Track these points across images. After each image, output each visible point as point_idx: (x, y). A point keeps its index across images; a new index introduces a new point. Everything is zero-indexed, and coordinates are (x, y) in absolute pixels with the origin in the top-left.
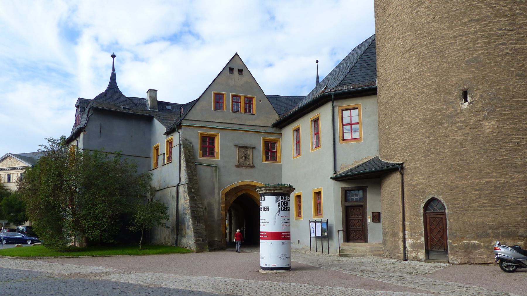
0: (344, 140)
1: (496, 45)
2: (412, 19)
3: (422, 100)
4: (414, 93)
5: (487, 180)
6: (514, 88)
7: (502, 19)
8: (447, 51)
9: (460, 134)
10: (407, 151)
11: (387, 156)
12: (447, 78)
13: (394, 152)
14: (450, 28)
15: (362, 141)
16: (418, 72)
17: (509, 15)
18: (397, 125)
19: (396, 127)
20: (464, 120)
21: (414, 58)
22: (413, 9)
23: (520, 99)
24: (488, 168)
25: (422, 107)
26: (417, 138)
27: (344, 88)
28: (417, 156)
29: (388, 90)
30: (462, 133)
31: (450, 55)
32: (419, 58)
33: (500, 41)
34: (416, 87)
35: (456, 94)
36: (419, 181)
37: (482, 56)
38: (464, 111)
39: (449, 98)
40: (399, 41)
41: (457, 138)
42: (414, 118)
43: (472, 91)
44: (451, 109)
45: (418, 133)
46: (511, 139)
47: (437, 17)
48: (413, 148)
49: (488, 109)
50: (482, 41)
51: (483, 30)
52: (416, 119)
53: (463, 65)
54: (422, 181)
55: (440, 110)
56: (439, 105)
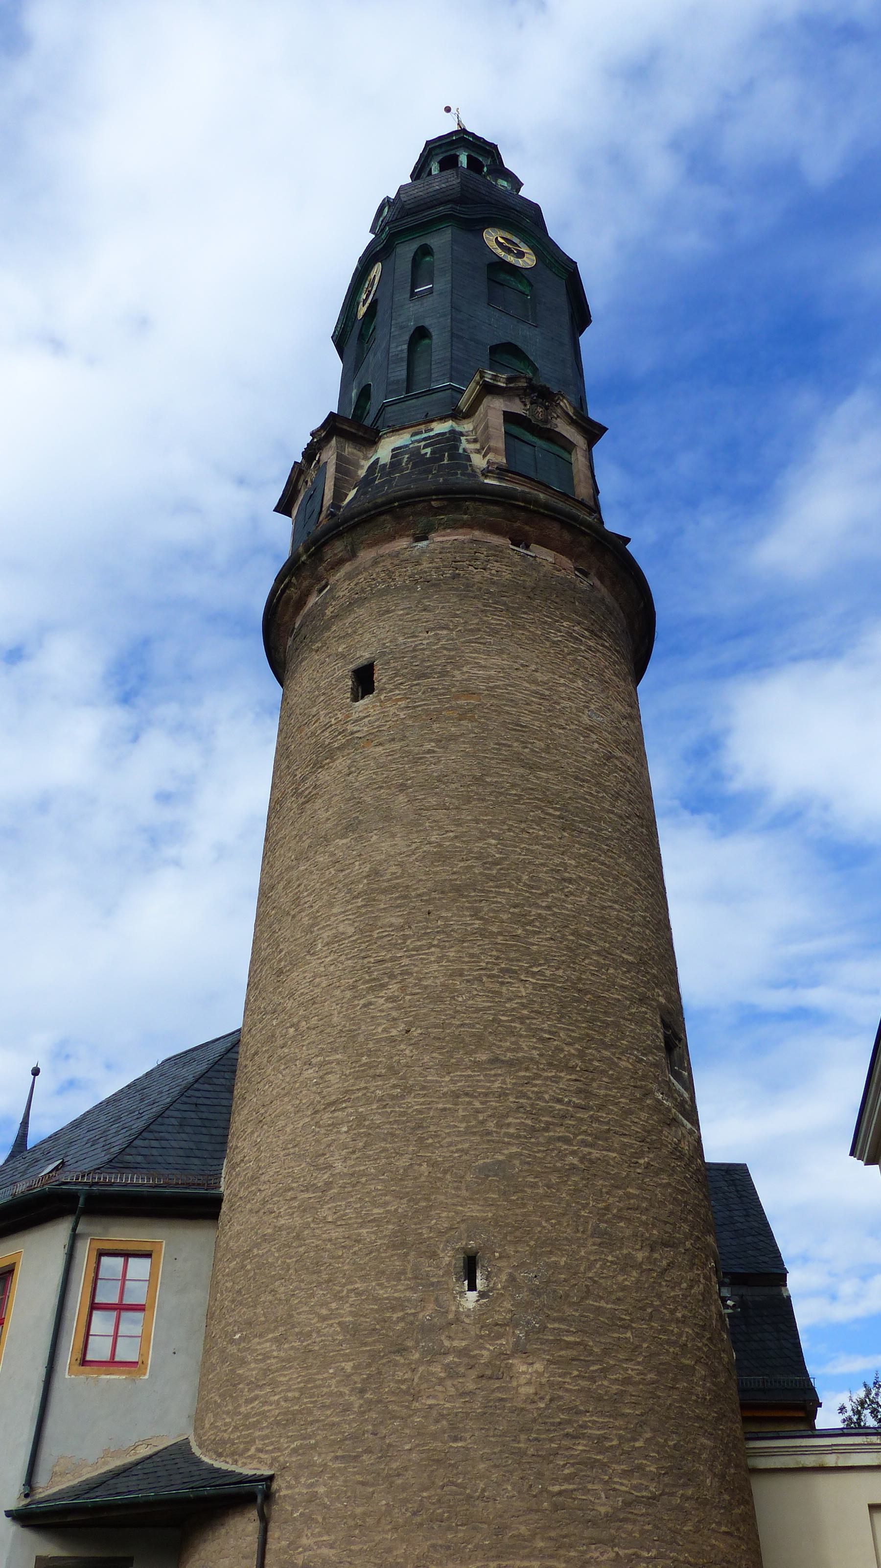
0: (84, 1362)
1: (550, 1140)
2: (352, 1019)
3: (354, 1264)
4: (334, 1235)
6: (589, 1268)
7: (562, 1074)
8: (432, 1128)
9: (452, 1391)
10: (292, 1430)
11: (223, 1442)
12: (426, 1207)
13: (248, 1429)
14: (445, 1067)
15: (145, 1374)
16: (352, 1175)
17: (578, 1069)
18: (270, 1336)
19: (266, 1341)
20: (465, 1348)
21: (345, 1129)
22: (356, 994)
23: (603, 1304)
24: (521, 1519)
25: (352, 1287)
26: (325, 1390)
27: (121, 1179)
28: (320, 1454)
29: (257, 1212)
30: (457, 1389)
31: (439, 1142)
32: (359, 1134)
34: (340, 1218)
35: (447, 1259)
36: (319, 1551)
37: (517, 1162)
38: (468, 1316)
39: (429, 1269)
40: (310, 1071)
41: (442, 1403)
42: (324, 1319)
43: (489, 1261)
44: (431, 1306)
45: (331, 1371)
46: (581, 1427)
47: (416, 1032)
48: (311, 1423)
49: (528, 1323)
50: (519, 1121)
51: (521, 1092)
52: (330, 1322)
53: (469, 1177)
54: (325, 1551)
55: (398, 1305)
56: (399, 1287)
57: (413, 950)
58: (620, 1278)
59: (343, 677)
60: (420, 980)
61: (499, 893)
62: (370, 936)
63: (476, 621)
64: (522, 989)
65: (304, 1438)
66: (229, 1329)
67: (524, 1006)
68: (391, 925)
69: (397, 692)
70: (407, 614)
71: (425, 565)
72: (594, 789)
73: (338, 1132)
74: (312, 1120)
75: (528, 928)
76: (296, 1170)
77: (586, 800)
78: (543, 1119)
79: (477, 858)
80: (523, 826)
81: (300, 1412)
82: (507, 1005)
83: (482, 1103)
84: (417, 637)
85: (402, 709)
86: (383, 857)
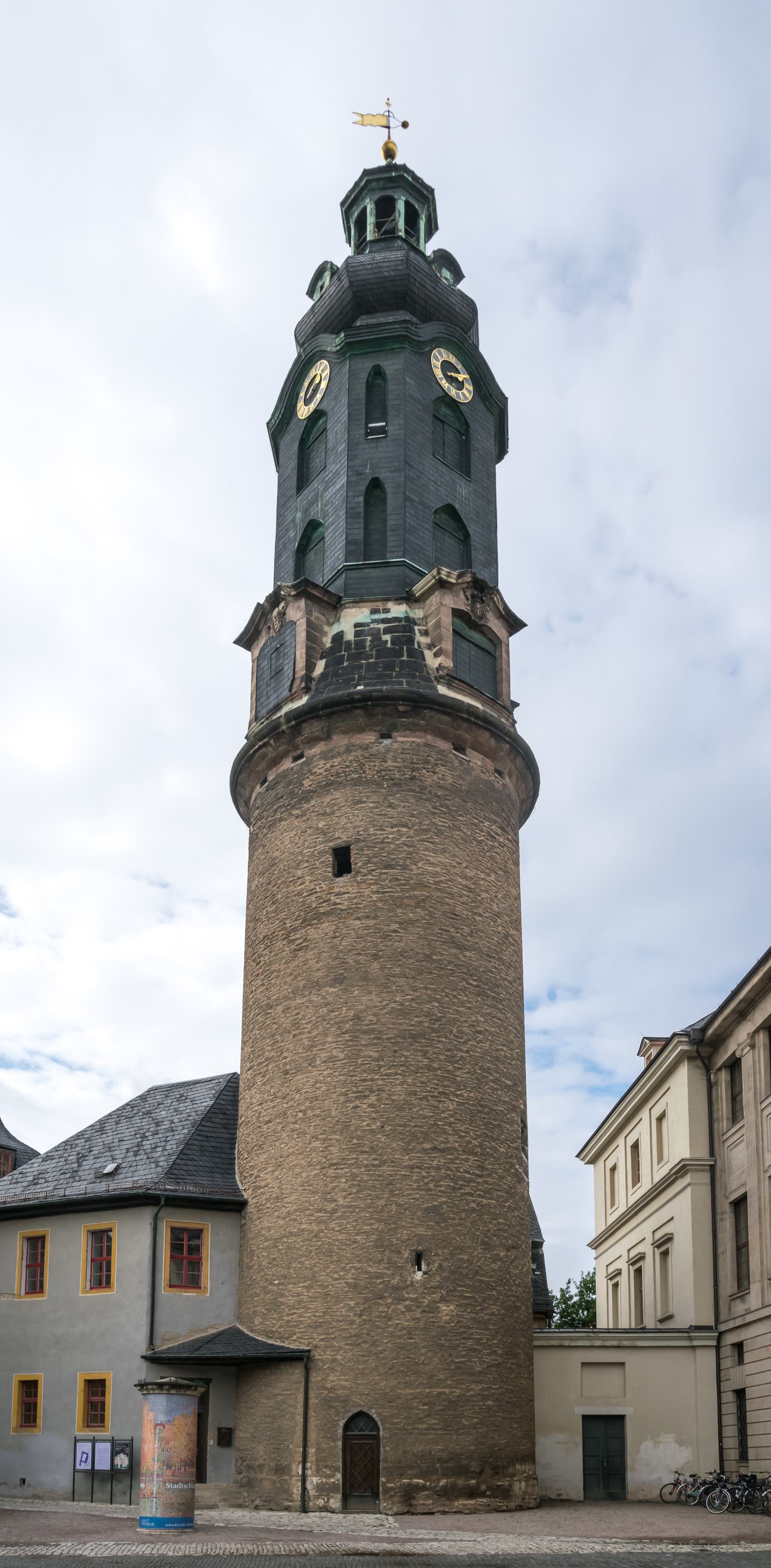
1: (463, 1194)
2: (346, 1115)
4: (340, 1238)
6: (478, 1261)
7: (470, 1157)
8: (398, 1185)
9: (408, 1317)
10: (319, 1330)
14: (406, 1151)
16: (350, 1207)
18: (301, 1285)
23: (484, 1278)
26: (339, 1313)
28: (337, 1342)
32: (353, 1184)
33: (466, 1188)
34: (343, 1229)
35: (406, 1255)
37: (445, 1206)
38: (417, 1283)
42: (336, 1279)
43: (429, 1256)
49: (448, 1287)
51: (448, 1167)
53: (419, 1213)
55: (380, 1276)
57: (385, 1075)
58: (493, 1266)
60: (390, 1095)
61: (439, 1041)
62: (356, 1062)
63: (427, 822)
64: (451, 1105)
65: (328, 1334)
67: (451, 1116)
68: (370, 1057)
69: (370, 877)
70: (377, 808)
71: (390, 763)
72: (497, 963)
73: (340, 1182)
74: (321, 1172)
75: (455, 1065)
76: (312, 1199)
77: (492, 972)
78: (460, 1183)
79: (426, 1016)
80: (455, 993)
81: (325, 1322)
82: (442, 1115)
83: (427, 1173)
84: (384, 830)
86: (363, 1007)
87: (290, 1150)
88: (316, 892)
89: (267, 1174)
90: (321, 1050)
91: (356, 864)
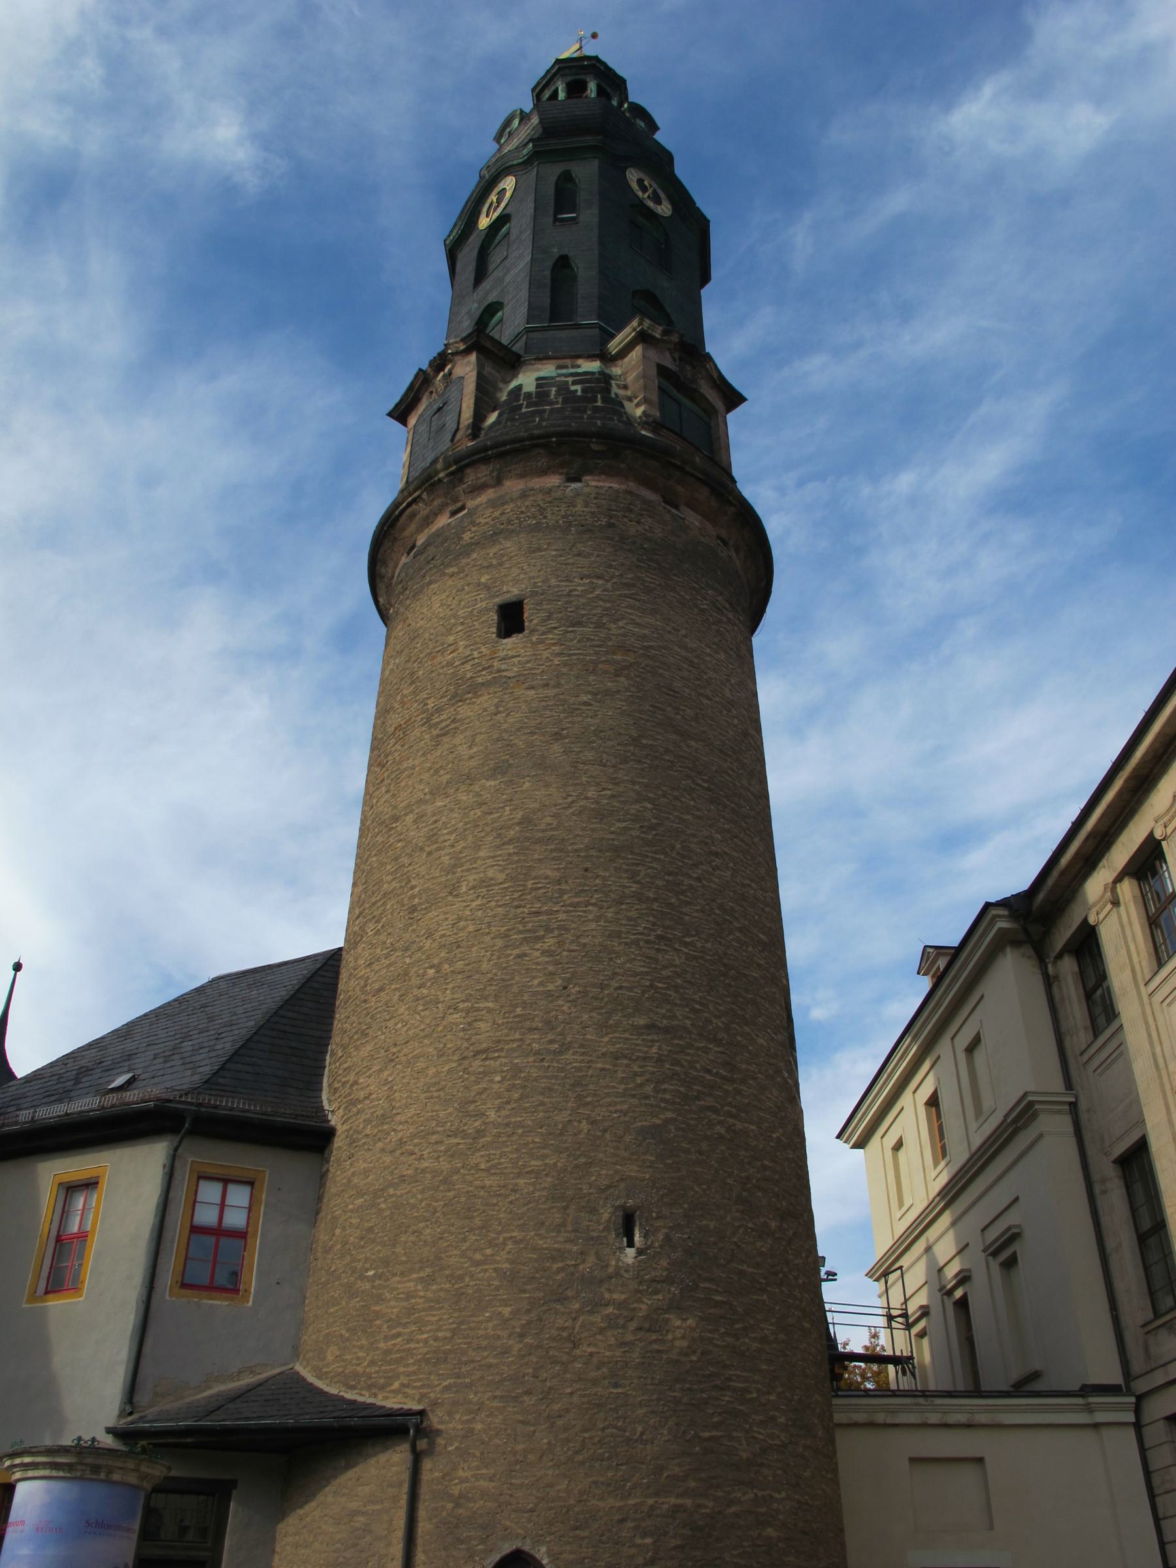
2: (505, 968)
3: (510, 1213)
4: (488, 1183)
5: (673, 1501)
7: (711, 1046)
9: (612, 1341)
11: (356, 1375)
12: (586, 1163)
13: (390, 1364)
15: (248, 1302)
16: (507, 1125)
17: (724, 1042)
18: (415, 1276)
19: (409, 1281)
20: (625, 1301)
21: (498, 1078)
22: (509, 943)
25: (509, 1235)
26: (481, 1332)
27: (227, 1102)
28: (476, 1393)
29: (392, 1152)
30: (616, 1339)
31: (598, 1101)
33: (708, 1099)
36: (477, 1484)
37: (672, 1127)
38: (627, 1271)
39: (589, 1223)
40: (455, 1016)
41: (603, 1351)
42: (478, 1264)
44: (592, 1259)
45: (487, 1314)
47: (574, 990)
50: (673, 1087)
52: (485, 1267)
56: (559, 1239)
57: (570, 905)
59: (487, 610)
60: (578, 937)
61: (655, 859)
62: (524, 885)
63: (630, 576)
64: (677, 958)
65: (458, 1377)
66: (359, 1265)
67: (678, 975)
68: (547, 877)
69: (551, 636)
70: (561, 556)
72: (735, 764)
73: (492, 1081)
74: (460, 1065)
75: (681, 897)
77: (729, 775)
78: (696, 1087)
79: (633, 820)
80: (676, 793)
82: (663, 972)
83: (640, 1067)
84: (571, 581)
85: (558, 655)
86: (537, 805)
87: (411, 1033)
88: (474, 659)
89: (369, 1077)
90: (468, 870)
91: (531, 621)
